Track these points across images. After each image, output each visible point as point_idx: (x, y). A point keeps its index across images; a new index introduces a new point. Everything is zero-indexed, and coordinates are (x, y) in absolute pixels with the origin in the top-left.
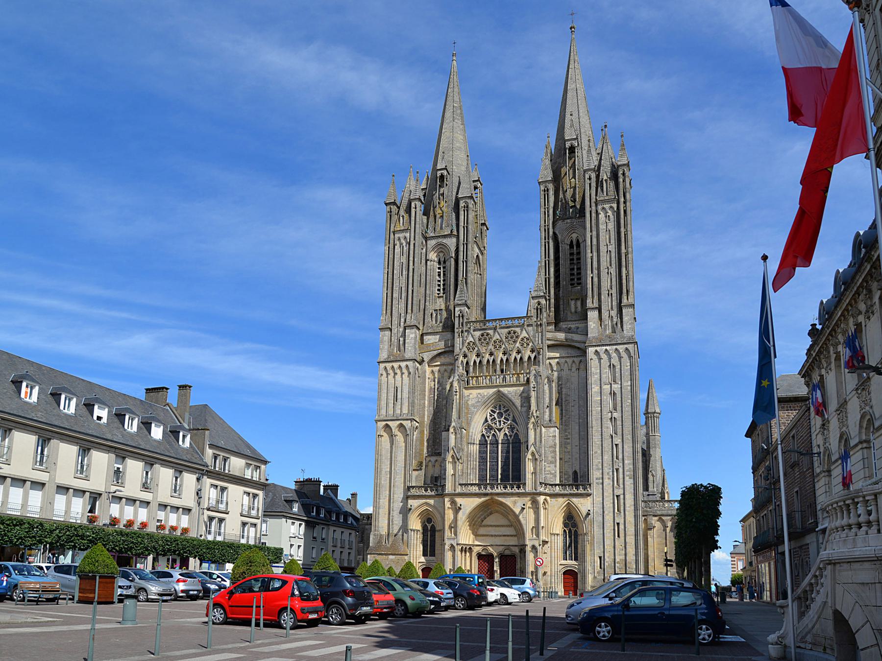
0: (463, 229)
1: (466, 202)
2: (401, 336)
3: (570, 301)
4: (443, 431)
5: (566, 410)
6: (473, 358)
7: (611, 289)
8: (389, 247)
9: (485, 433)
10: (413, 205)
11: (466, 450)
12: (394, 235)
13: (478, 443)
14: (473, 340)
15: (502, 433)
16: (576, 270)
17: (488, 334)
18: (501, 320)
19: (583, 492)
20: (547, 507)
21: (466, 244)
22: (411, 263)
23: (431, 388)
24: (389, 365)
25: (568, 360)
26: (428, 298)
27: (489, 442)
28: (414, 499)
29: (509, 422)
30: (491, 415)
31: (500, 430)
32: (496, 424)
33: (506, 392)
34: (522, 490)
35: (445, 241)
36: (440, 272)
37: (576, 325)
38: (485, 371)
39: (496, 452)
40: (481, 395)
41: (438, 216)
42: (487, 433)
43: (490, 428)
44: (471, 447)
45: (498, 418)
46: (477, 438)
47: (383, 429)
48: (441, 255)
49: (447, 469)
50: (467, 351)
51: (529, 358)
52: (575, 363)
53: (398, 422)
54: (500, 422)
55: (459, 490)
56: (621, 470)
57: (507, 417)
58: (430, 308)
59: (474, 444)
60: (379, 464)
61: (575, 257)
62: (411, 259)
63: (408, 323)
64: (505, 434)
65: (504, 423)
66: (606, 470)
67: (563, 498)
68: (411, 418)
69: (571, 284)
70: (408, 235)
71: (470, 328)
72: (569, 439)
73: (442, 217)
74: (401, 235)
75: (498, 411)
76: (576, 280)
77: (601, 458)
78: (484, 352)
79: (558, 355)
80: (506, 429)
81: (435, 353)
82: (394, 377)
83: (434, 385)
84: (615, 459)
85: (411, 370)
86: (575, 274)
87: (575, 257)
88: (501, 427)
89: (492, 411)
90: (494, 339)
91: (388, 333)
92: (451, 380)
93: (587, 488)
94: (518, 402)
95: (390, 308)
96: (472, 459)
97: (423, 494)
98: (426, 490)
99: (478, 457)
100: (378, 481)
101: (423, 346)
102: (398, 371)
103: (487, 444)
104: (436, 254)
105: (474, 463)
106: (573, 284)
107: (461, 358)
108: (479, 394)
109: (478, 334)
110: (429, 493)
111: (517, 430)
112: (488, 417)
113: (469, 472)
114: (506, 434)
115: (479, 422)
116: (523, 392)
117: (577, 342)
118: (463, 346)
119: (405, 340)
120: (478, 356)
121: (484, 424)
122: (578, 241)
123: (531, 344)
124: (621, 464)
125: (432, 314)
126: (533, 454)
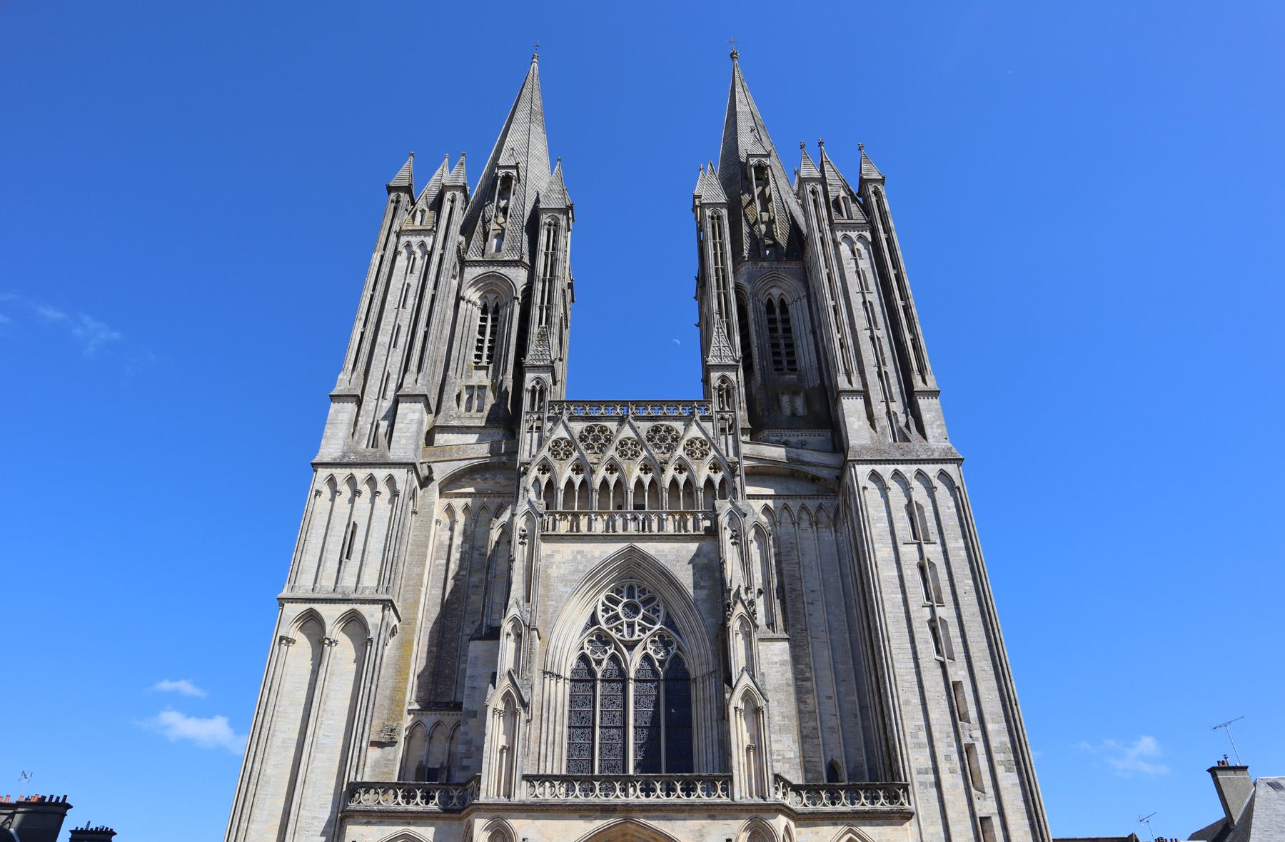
0: (543, 257)
1: (553, 217)
2: (384, 418)
3: (780, 394)
4: (472, 639)
6: (564, 472)
7: (884, 364)
8: (382, 257)
9: (588, 652)
10: (448, 195)
11: (537, 689)
12: (398, 237)
13: (568, 675)
16: (783, 346)
17: (603, 430)
18: (637, 403)
19: (888, 807)
21: (550, 281)
22: (430, 285)
23: (441, 544)
24: (341, 474)
25: (790, 503)
26: (453, 365)
27: (599, 676)
28: (368, 823)
29: (657, 627)
30: (606, 610)
31: (631, 646)
32: (621, 631)
34: (719, 798)
35: (503, 271)
36: (485, 326)
37: (800, 438)
38: (595, 504)
39: (620, 701)
41: (491, 233)
42: (593, 652)
43: (602, 640)
44: (551, 684)
45: (627, 615)
46: (567, 664)
47: (300, 624)
48: (491, 297)
49: (488, 731)
50: (551, 458)
51: (709, 482)
52: (808, 512)
53: (345, 608)
54: (631, 626)
55: (522, 793)
56: (980, 748)
57: (650, 614)
58: (457, 384)
60: (268, 718)
61: (779, 326)
62: (432, 277)
63: (408, 387)
64: (646, 658)
65: (643, 630)
66: (941, 749)
67: (835, 824)
68: (385, 597)
69: (776, 370)
70: (429, 240)
71: (561, 413)
72: (807, 679)
73: (500, 237)
74: (415, 240)
75: (625, 600)
76: (785, 363)
77: (921, 715)
78: (595, 461)
79: (771, 492)
80: (649, 645)
81: (464, 464)
82: (352, 501)
83: (451, 539)
84: (959, 723)
85: (400, 486)
86: (783, 352)
87: (779, 326)
88: (635, 637)
89: (609, 598)
90: (622, 436)
91: (351, 407)
92: (505, 517)
93: (897, 797)
94: (685, 577)
95: (365, 359)
97: (399, 808)
98: (409, 797)
99: (566, 713)
100: (257, 766)
101: (430, 449)
102: (365, 490)
103: (594, 681)
104: (479, 294)
105: (558, 729)
106: (782, 370)
107: (534, 472)
108: (579, 552)
109: (578, 427)
110: (418, 805)
111: (679, 648)
112: (600, 613)
113: (543, 751)
115: (574, 623)
116: (696, 555)
117: (809, 464)
118: (540, 445)
119: (392, 426)
120: (578, 469)
121: (586, 629)
122: (782, 302)
123: (712, 453)
124: (977, 734)
125: (459, 396)
126: (747, 696)
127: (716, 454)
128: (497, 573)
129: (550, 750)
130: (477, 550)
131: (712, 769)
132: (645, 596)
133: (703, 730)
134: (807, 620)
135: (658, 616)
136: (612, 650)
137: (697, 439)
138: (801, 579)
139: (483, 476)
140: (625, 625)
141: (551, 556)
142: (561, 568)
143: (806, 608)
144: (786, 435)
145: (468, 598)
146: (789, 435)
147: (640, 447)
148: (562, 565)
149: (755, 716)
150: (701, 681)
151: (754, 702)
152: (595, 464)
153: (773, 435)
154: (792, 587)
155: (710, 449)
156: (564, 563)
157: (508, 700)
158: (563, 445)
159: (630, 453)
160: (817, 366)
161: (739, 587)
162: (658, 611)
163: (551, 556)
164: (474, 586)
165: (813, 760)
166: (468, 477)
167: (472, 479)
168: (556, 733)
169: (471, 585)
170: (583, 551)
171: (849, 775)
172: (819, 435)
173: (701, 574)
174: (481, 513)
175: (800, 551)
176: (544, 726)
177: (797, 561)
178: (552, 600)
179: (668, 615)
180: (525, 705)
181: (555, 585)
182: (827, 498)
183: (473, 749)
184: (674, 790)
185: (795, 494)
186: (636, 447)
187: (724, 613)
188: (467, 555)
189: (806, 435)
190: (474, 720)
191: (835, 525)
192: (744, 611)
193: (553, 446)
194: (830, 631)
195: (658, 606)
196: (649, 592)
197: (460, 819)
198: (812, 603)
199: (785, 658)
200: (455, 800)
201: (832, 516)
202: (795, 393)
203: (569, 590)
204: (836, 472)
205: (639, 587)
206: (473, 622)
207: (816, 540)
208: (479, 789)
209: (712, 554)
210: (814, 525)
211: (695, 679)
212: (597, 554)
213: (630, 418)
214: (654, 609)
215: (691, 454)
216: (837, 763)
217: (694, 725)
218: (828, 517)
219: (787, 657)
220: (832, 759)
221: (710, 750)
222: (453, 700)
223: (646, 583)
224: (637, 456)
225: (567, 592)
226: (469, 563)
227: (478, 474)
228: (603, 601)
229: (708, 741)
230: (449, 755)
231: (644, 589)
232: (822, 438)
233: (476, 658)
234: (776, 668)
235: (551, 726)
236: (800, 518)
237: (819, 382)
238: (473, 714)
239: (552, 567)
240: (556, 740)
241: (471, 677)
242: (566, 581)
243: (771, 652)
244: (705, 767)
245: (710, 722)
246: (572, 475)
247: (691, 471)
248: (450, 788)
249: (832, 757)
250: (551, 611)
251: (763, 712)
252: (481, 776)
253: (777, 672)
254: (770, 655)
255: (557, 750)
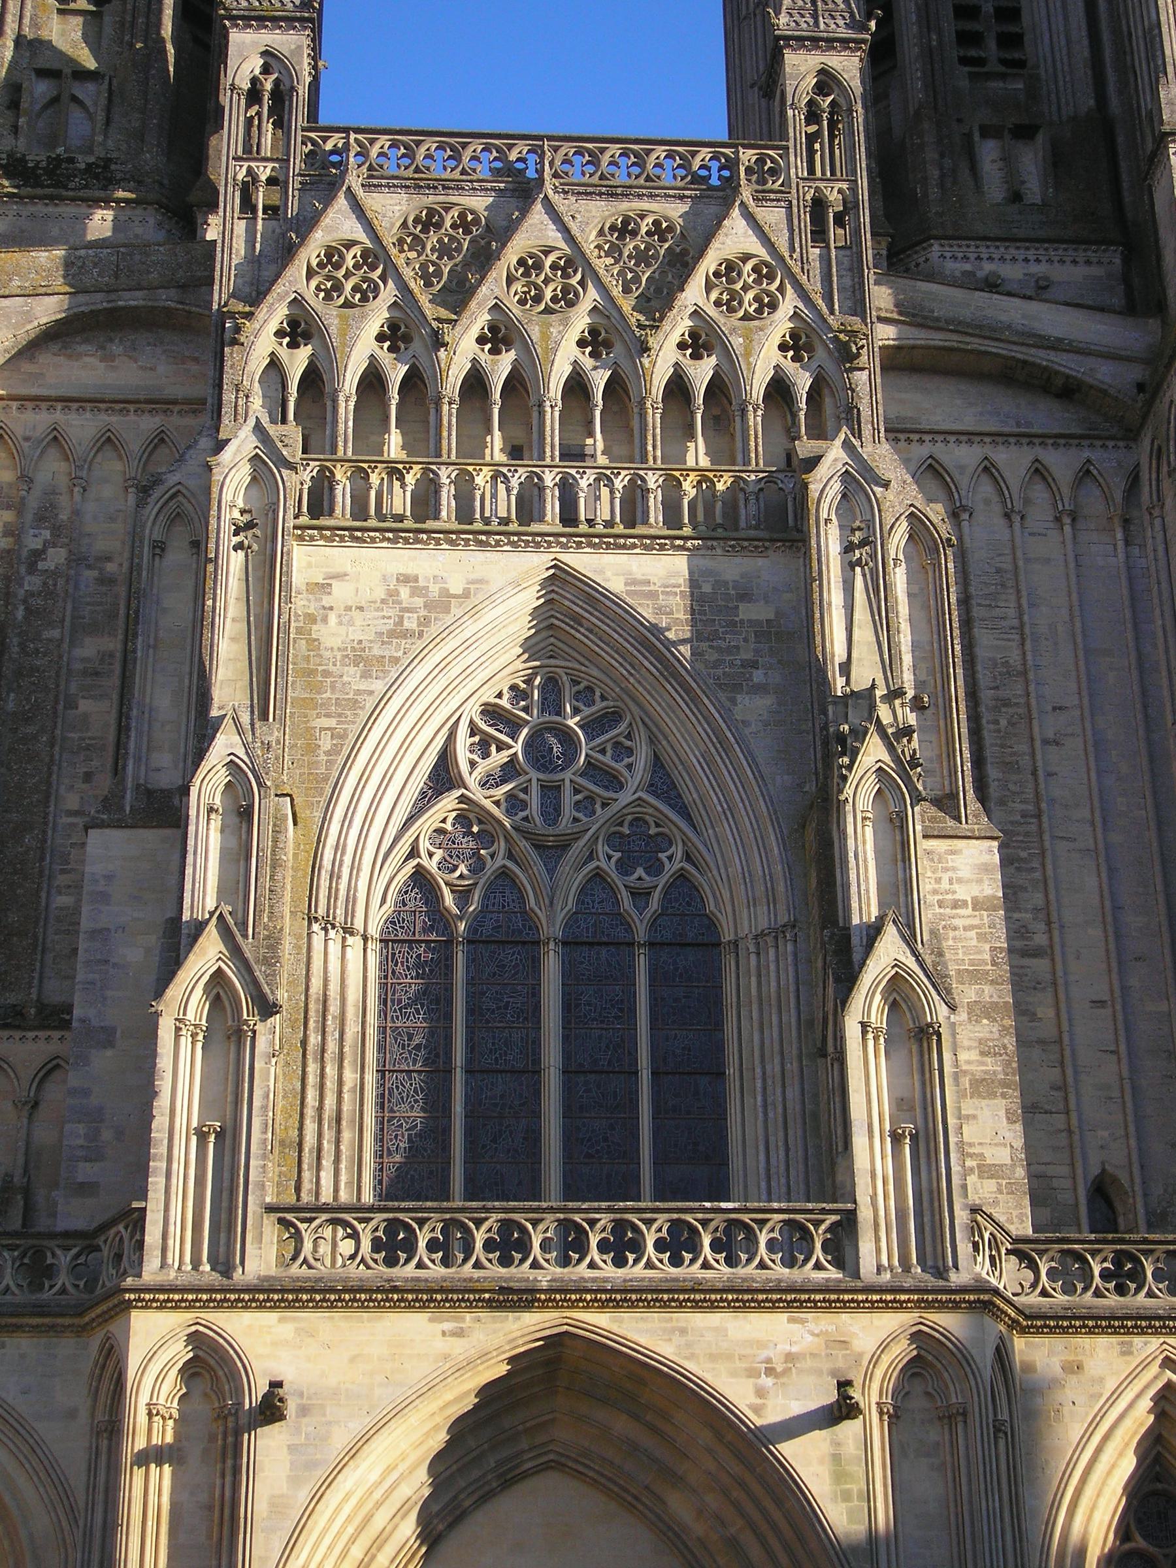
3: (976, 137)
4: (94, 824)
5: (1009, 767)
9: (432, 865)
13: (374, 930)
14: (360, 235)
15: (570, 877)
20: (1004, 1415)
25: (1002, 456)
33: (616, 585)
37: (1034, 268)
40: (415, 591)
57: (607, 759)
59: (348, 931)
65: (586, 804)
69: (964, 61)
72: (1036, 953)
80: (601, 848)
96: (332, 1046)
105: (350, 1076)
108: (405, 579)
111: (688, 857)
112: (463, 754)
114: (598, 876)
127: (801, 305)
128: (161, 634)
129: (328, 1135)
130: (89, 567)
131: (784, 1190)
132: (594, 709)
133: (759, 1084)
134: (1042, 786)
135: (629, 767)
136: (500, 861)
137: (746, 258)
138: (1025, 673)
139: (103, 348)
140: (535, 788)
141: (323, 588)
142: (351, 623)
143: (1039, 757)
144: (990, 259)
145: (71, 704)
146: (1002, 259)
147: (579, 276)
148: (355, 613)
149: (915, 1048)
150: (752, 949)
151: (916, 1010)
152: (449, 321)
153: (954, 257)
154: (1001, 693)
155: (781, 288)
156: (361, 609)
157: (218, 996)
158: (350, 263)
159: (548, 294)
160: (1086, 53)
161: (873, 687)
162: (630, 752)
163: (323, 588)
164: (85, 673)
165: (1050, 1170)
166: (55, 347)
167: (70, 357)
168: (346, 1089)
169: (77, 666)
170: (416, 579)
171: (1147, 1213)
172: (1088, 262)
173: (756, 651)
174: (100, 455)
175: (1024, 593)
176: (312, 1068)
177: (1016, 623)
178: (328, 716)
179: (657, 762)
180: (268, 1009)
181: (331, 668)
182: (1103, 446)
183: (107, 1135)
184: (695, 1249)
185: (1016, 430)
186: (566, 275)
187: (828, 759)
188: (61, 582)
189: (1050, 261)
190: (109, 1053)
191: (1126, 522)
192: (886, 758)
193: (321, 265)
194: (1105, 822)
195: (629, 737)
196: (603, 698)
197: (82, 1331)
198: (1057, 744)
199: (988, 891)
200: (63, 1279)
201: (1118, 496)
202: (1024, 132)
203: (379, 686)
204: (1136, 373)
205: (575, 683)
206: (88, 777)
207: (1072, 565)
208: (140, 1245)
209: (787, 596)
210: (1067, 520)
211: (736, 944)
212: (456, 588)
213: (548, 188)
214: (617, 744)
215: (730, 304)
216: (1115, 1180)
217: (732, 1071)
218: (1107, 499)
219: (992, 888)
220: (1104, 1170)
221: (776, 1140)
222: (34, 996)
223: (595, 672)
224: (571, 304)
225: (371, 693)
226: (69, 607)
227: (86, 341)
228: (471, 721)
229: (771, 1115)
230: (26, 1154)
231: (589, 689)
232: (1095, 271)
233: (109, 878)
234: (965, 917)
235: (331, 1071)
236: (1027, 501)
237: (1092, 102)
238: (106, 1037)
239: (325, 620)
240: (346, 1107)
241: (94, 934)
242: (367, 661)
243: (950, 874)
244: (763, 1184)
245: (777, 1060)
246: (378, 352)
247: (727, 353)
248: (45, 1243)
249: (1103, 1163)
250: (326, 743)
251: (939, 1035)
252: (145, 1209)
253: (965, 929)
254: (945, 885)
255: (346, 1135)
